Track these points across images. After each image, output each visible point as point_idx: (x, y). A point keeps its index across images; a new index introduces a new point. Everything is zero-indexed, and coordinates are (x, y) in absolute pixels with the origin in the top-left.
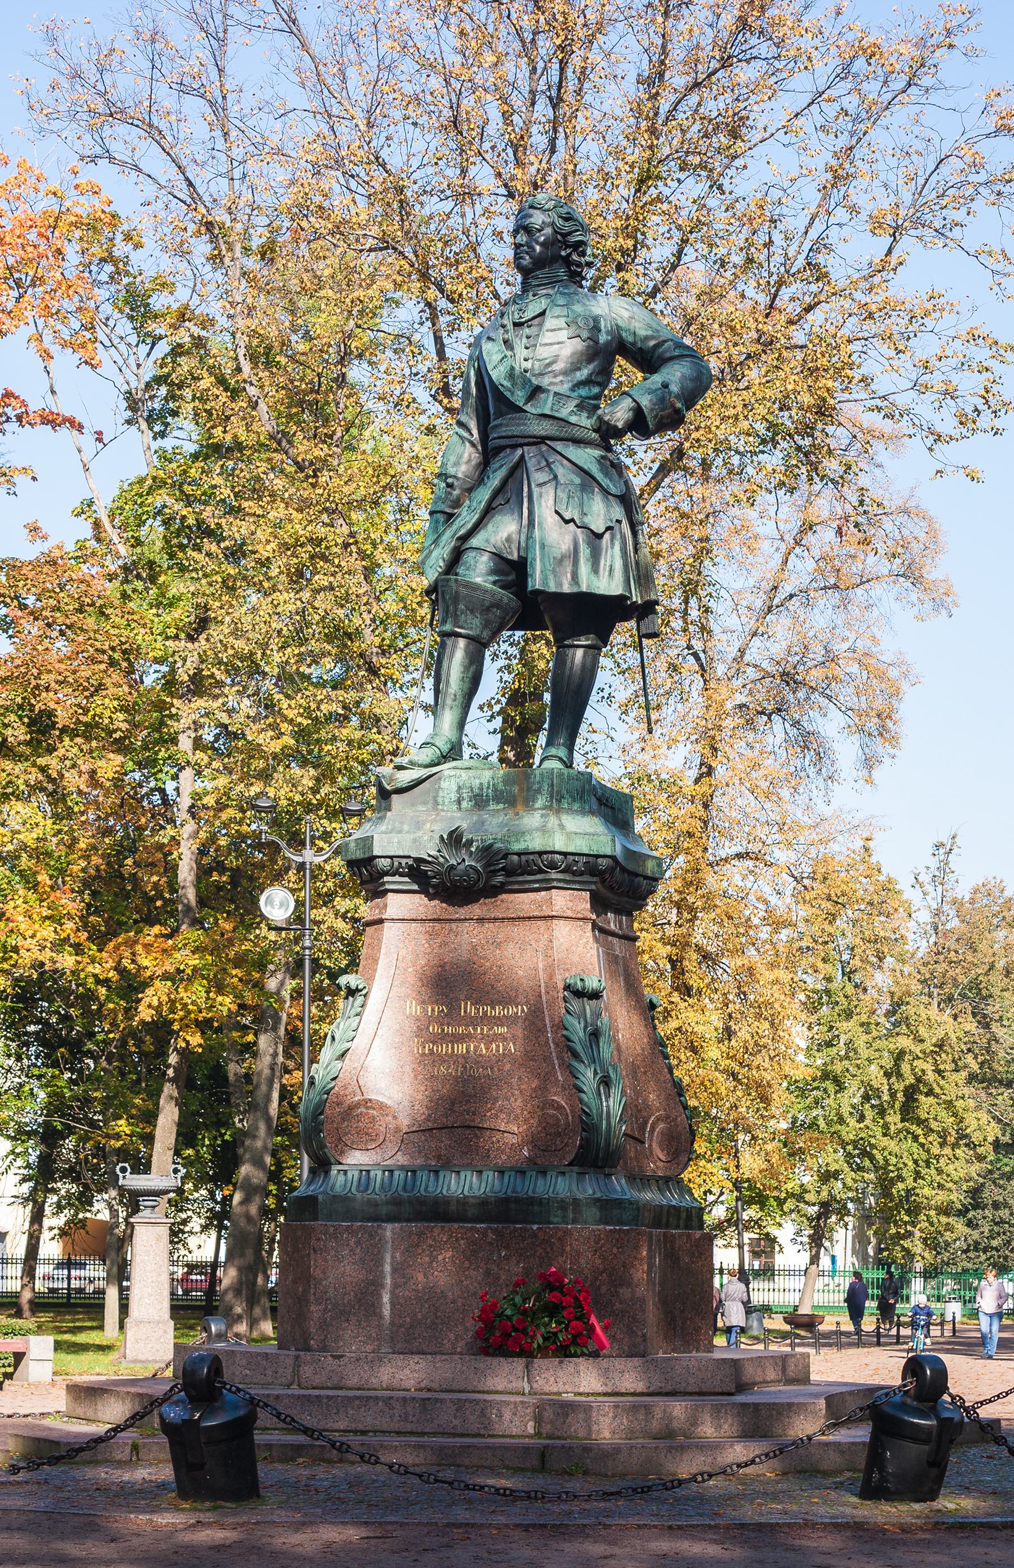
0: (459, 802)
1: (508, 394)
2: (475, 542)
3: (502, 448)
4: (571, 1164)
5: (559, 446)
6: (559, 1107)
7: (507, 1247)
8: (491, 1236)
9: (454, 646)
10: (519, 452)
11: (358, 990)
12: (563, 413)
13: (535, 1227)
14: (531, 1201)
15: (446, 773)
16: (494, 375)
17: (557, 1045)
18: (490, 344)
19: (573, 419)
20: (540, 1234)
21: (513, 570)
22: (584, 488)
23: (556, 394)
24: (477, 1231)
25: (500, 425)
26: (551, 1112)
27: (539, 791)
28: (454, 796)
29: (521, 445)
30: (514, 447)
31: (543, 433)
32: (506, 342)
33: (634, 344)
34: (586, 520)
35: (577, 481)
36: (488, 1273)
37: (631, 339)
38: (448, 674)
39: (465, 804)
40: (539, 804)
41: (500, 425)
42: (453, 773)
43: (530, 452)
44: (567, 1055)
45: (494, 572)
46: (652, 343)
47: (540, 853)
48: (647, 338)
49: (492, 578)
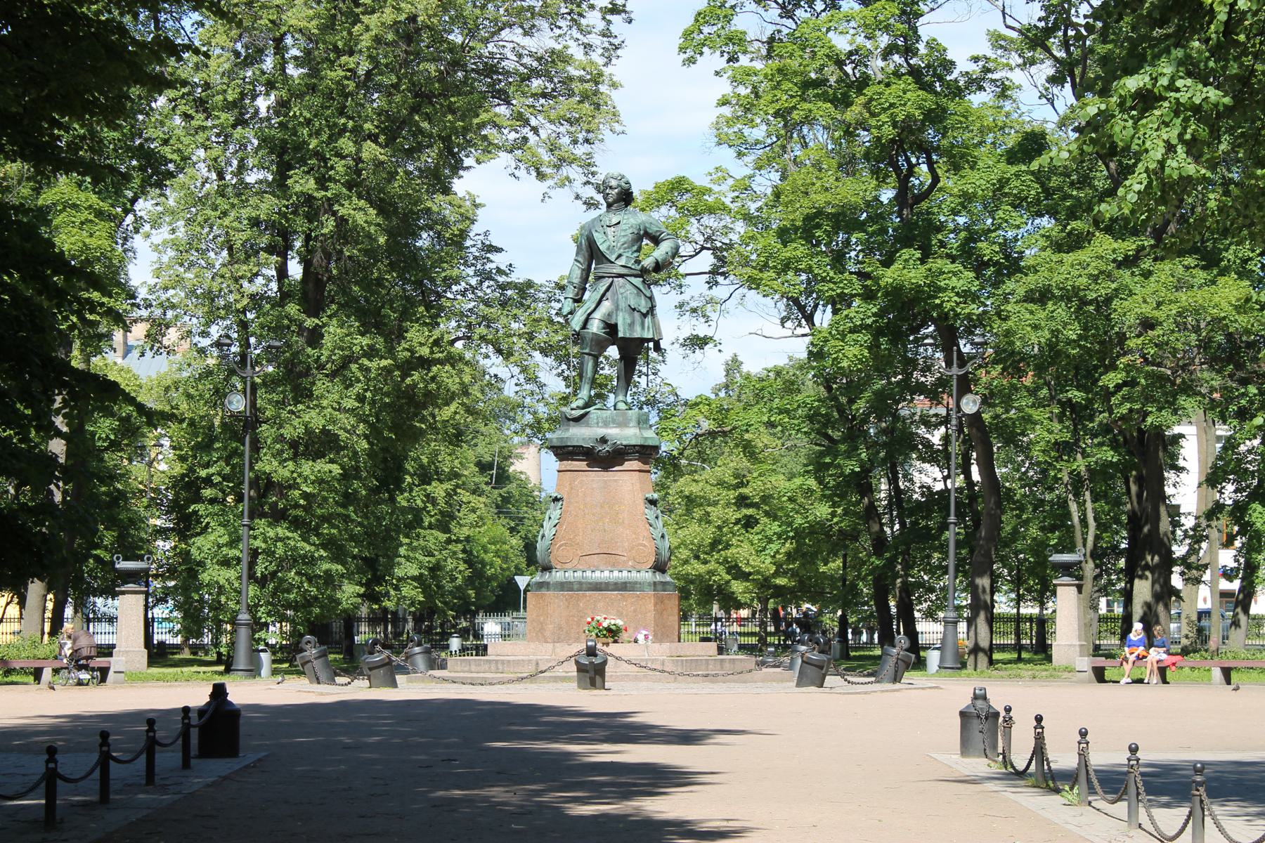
2: (594, 315)
14: (636, 583)
21: (611, 328)
22: (638, 295)
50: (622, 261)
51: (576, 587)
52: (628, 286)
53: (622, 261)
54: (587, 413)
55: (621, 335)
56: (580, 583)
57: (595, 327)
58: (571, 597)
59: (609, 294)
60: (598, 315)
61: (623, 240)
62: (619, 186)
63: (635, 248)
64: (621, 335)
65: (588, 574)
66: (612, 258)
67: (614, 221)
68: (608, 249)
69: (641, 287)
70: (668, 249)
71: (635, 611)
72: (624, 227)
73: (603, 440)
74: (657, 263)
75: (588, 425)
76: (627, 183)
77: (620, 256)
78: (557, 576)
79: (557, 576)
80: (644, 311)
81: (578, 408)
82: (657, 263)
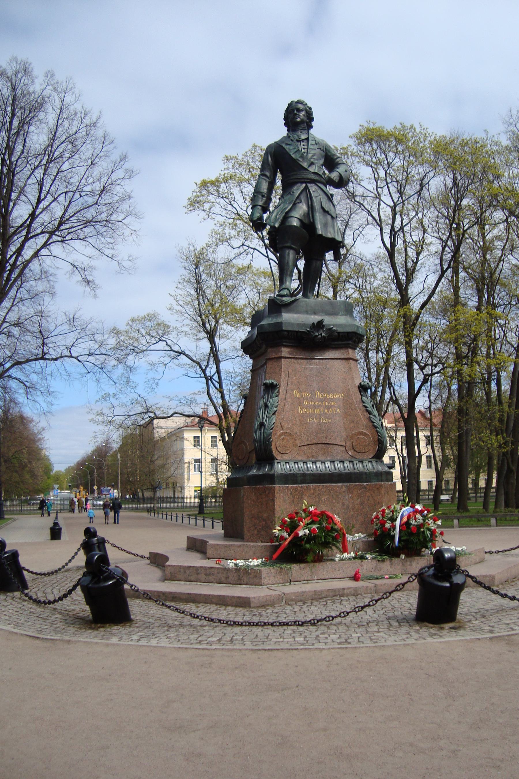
1: (301, 163)
3: (295, 183)
4: (372, 458)
6: (365, 435)
7: (352, 493)
8: (344, 488)
9: (289, 253)
10: (304, 185)
11: (276, 385)
13: (365, 484)
16: (293, 156)
17: (360, 410)
20: (368, 487)
24: (338, 487)
26: (362, 436)
29: (306, 183)
30: (302, 183)
33: (330, 156)
36: (343, 504)
38: (288, 262)
43: (309, 185)
44: (367, 414)
45: (301, 226)
51: (299, 479)
52: (320, 191)
54: (296, 300)
55: (320, 232)
56: (304, 475)
57: (295, 223)
58: (296, 490)
59: (303, 198)
61: (313, 152)
65: (310, 465)
66: (305, 165)
67: (303, 137)
71: (362, 504)
74: (341, 176)
75: (297, 312)
76: (310, 108)
77: (312, 164)
78: (279, 468)
79: (279, 468)
82: (341, 176)
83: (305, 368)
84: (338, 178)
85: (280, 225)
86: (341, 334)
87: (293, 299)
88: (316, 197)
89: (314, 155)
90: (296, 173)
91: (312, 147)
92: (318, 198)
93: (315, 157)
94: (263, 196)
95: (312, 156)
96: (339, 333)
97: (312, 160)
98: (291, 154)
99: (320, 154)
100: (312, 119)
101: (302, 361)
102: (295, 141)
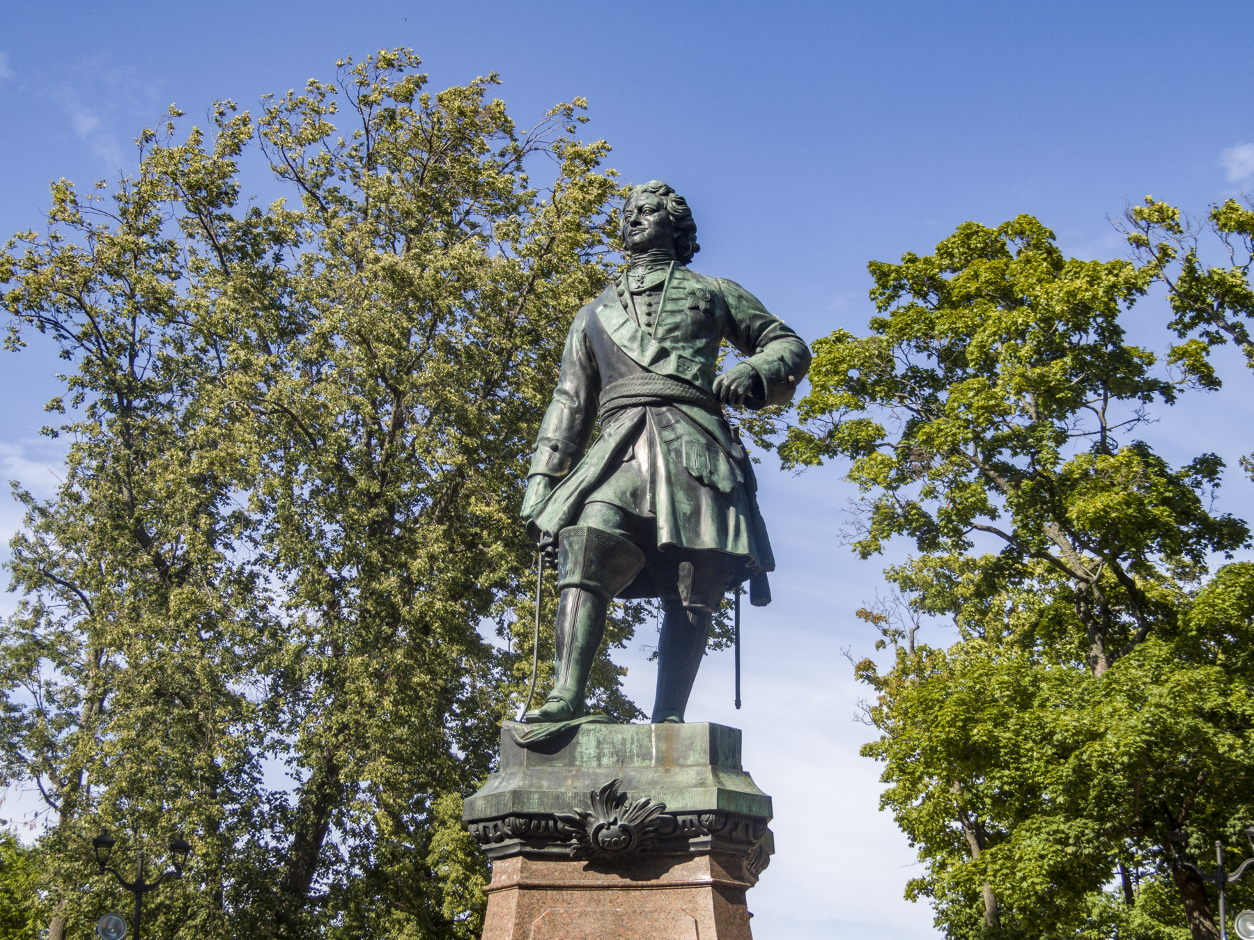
0: (599, 758)
2: (597, 495)
5: (684, 408)
12: (688, 376)
15: (584, 727)
16: (616, 338)
18: (607, 311)
19: (698, 383)
23: (680, 357)
25: (622, 385)
27: (691, 746)
28: (592, 751)
29: (644, 405)
31: (669, 392)
32: (625, 307)
33: (741, 321)
34: (715, 478)
35: (703, 441)
37: (740, 316)
39: (605, 761)
40: (690, 761)
41: (622, 385)
42: (592, 726)
46: (758, 323)
47: (699, 813)
48: (755, 317)
49: (618, 531)
50: (669, 366)
52: (682, 428)
53: (669, 366)
60: (607, 492)
61: (671, 320)
62: (659, 207)
63: (700, 343)
64: (664, 537)
68: (633, 338)
69: (718, 432)
70: (787, 356)
72: (674, 294)
73: (612, 797)
76: (681, 201)
77: (662, 354)
80: (725, 486)
81: (546, 717)
83: (583, 914)
84: (747, 382)
85: (562, 527)
86: (680, 819)
87: (554, 727)
88: (668, 443)
89: (676, 327)
90: (620, 381)
91: (670, 307)
92: (675, 445)
93: (677, 333)
94: (555, 448)
95: (670, 331)
96: (675, 814)
97: (667, 344)
98: (609, 330)
99: (694, 322)
100: (693, 229)
101: (576, 894)
102: (627, 295)
